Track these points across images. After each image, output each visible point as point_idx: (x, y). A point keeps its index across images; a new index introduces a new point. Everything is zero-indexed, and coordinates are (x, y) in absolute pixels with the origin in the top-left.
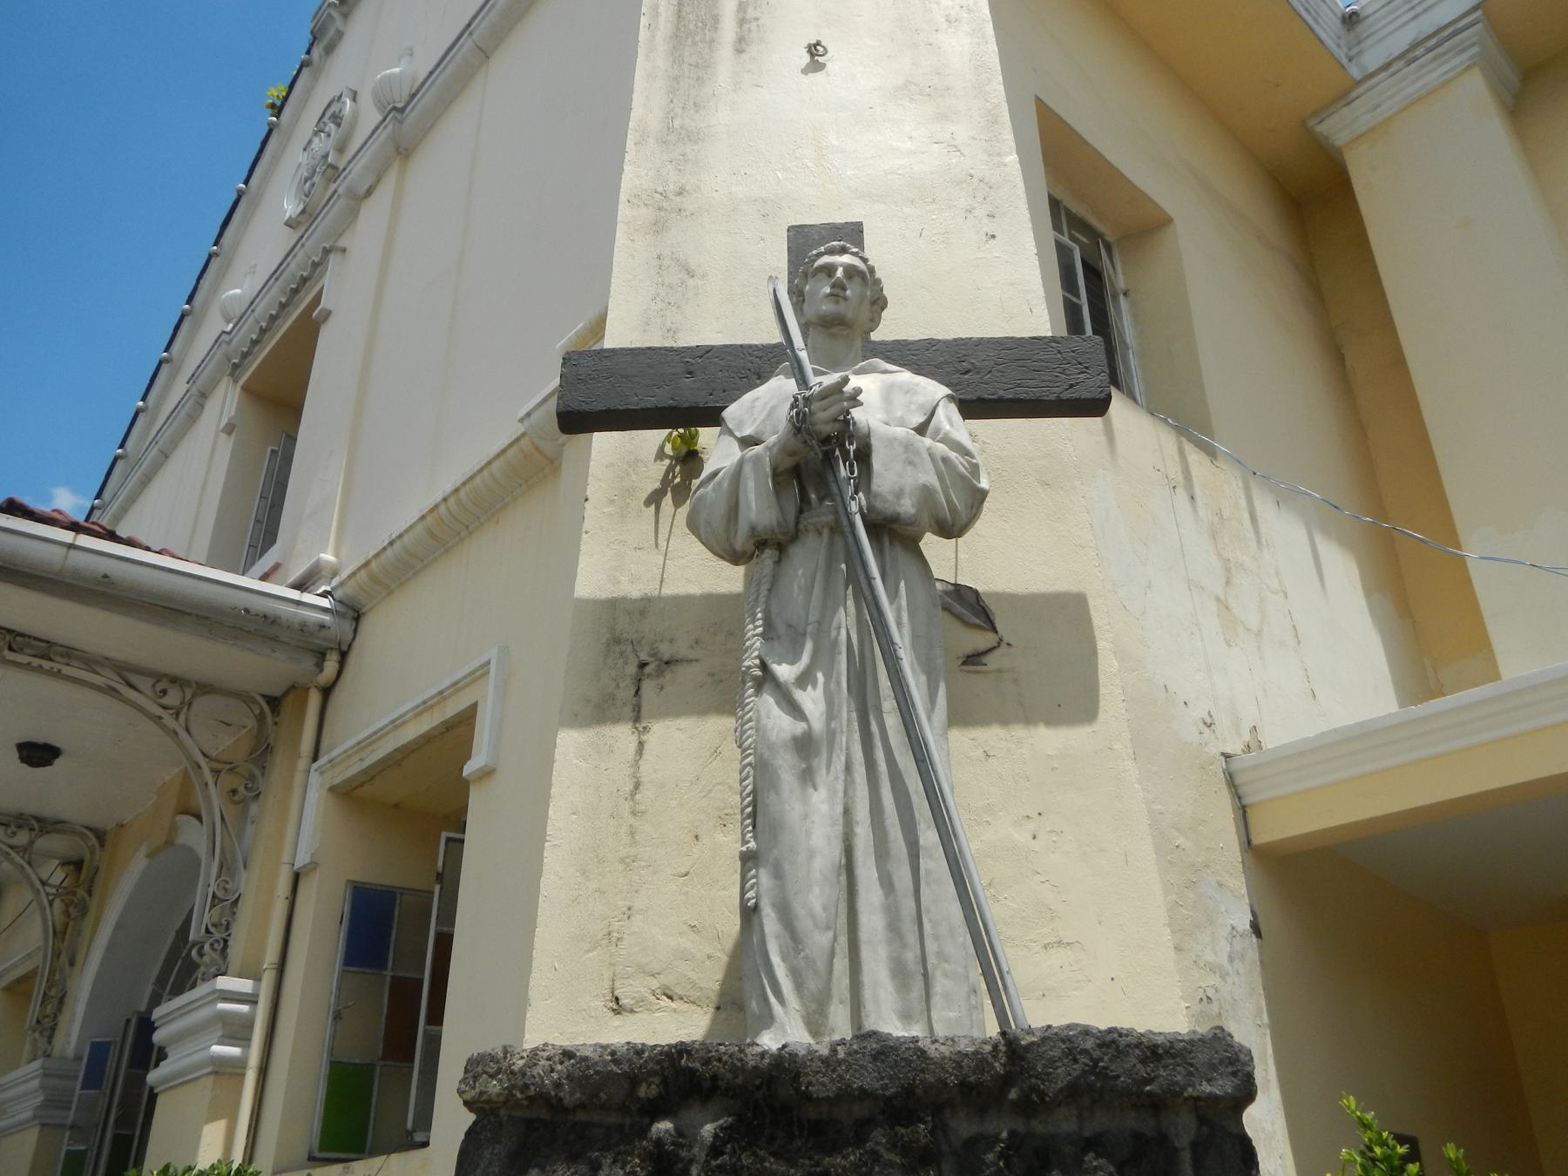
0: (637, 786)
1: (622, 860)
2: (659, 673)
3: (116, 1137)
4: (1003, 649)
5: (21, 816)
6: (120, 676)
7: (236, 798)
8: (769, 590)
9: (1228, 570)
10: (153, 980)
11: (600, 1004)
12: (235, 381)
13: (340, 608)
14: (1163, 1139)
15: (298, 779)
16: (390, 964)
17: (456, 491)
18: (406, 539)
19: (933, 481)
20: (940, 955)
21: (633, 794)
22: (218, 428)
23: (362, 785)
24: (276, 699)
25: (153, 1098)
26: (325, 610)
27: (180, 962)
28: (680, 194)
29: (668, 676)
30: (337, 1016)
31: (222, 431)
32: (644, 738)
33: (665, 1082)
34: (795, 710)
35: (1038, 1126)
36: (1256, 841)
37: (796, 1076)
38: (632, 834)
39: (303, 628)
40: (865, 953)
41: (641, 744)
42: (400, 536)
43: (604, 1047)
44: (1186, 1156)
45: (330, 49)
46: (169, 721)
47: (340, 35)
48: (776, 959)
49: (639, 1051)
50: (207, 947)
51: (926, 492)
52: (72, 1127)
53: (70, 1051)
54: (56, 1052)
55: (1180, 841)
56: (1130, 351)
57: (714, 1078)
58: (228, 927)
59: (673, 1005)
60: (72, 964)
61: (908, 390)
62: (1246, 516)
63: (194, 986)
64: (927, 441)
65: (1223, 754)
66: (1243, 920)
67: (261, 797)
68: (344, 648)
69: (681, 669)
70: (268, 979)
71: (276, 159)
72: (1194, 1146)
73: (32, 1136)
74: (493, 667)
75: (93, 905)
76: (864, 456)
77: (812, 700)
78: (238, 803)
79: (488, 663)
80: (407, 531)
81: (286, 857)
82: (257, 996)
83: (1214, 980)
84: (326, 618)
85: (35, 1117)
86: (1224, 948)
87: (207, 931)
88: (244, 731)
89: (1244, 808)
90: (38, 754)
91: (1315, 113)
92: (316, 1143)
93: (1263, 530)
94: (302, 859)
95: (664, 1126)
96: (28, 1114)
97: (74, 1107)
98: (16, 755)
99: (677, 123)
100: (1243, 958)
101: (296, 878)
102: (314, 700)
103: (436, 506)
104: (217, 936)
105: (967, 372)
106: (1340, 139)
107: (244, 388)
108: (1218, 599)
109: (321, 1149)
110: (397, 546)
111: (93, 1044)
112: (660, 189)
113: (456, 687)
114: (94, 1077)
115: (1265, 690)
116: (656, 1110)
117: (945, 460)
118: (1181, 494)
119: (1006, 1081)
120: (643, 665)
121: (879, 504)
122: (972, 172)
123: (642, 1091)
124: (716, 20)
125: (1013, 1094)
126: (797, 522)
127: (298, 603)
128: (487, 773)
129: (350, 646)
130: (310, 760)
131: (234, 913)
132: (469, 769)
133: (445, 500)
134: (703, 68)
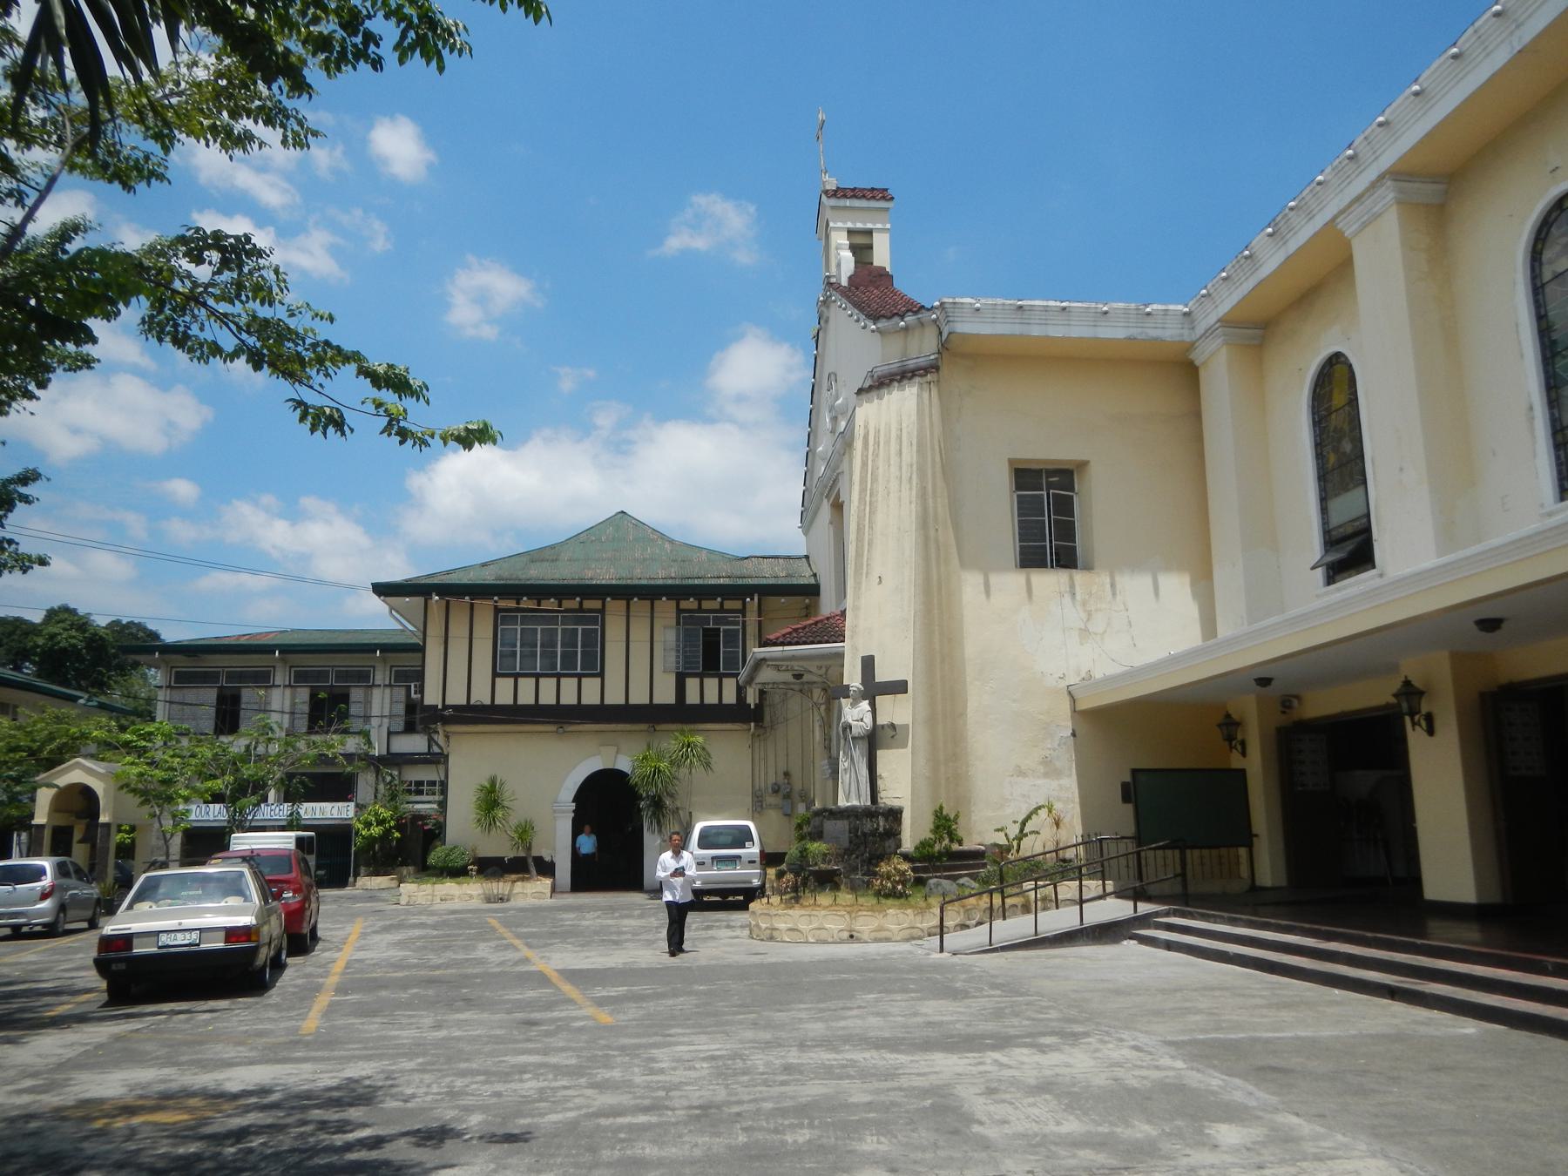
36: (1077, 709)
45: (827, 321)
47: (828, 318)
55: (1041, 717)
62: (1108, 586)
71: (822, 366)
89: (1074, 701)
91: (1187, 350)
93: (1118, 587)
100: (1065, 744)
106: (1197, 363)
118: (1067, 598)
124: (862, 564)
134: (860, 583)
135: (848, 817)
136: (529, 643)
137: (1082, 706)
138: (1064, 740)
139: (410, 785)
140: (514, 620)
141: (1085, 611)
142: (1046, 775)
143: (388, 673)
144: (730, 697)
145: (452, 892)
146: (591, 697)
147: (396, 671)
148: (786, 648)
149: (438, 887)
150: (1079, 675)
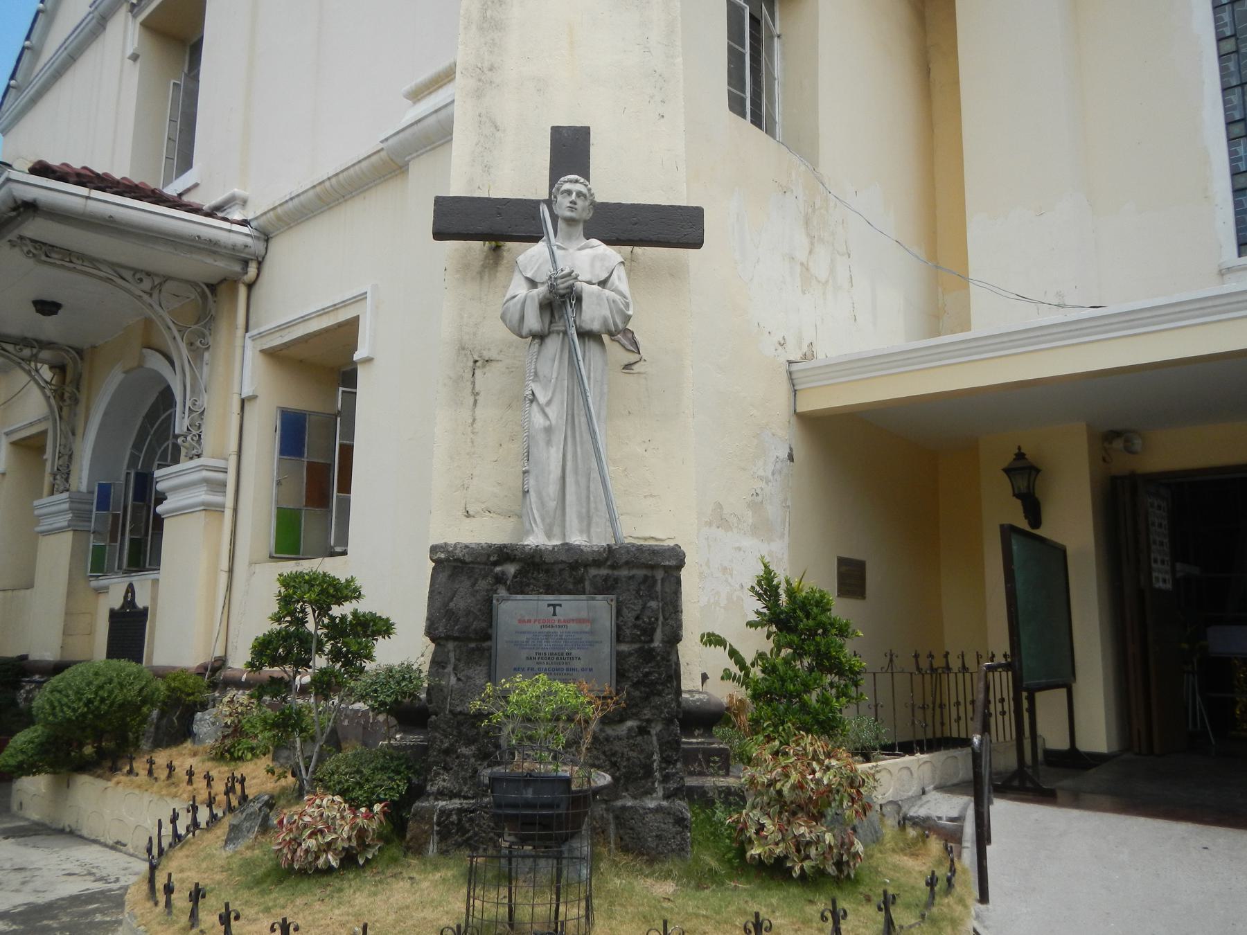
0: (474, 420)
1: (468, 454)
2: (484, 366)
3: (131, 540)
4: (641, 363)
5: (25, 339)
6: (116, 272)
7: (192, 347)
8: (537, 359)
9: (812, 244)
10: (130, 446)
11: (461, 513)
12: (135, 17)
13: (256, 233)
14: (653, 577)
15: (239, 342)
16: (306, 455)
17: (337, 174)
18: (302, 197)
19: (608, 314)
20: (596, 509)
21: (472, 424)
22: (123, 51)
23: (281, 350)
24: (212, 285)
25: (159, 522)
26: (247, 235)
27: (150, 437)
28: (490, 70)
29: (488, 368)
30: (279, 483)
31: (130, 58)
32: (477, 398)
33: (499, 556)
34: (546, 415)
35: (616, 573)
36: (798, 411)
37: (541, 557)
38: (472, 442)
39: (234, 247)
40: (568, 510)
41: (476, 401)
42: (298, 195)
43: (479, 544)
44: (659, 582)
46: (146, 297)
48: (535, 511)
49: (490, 546)
50: (189, 438)
51: (605, 321)
52: (94, 532)
53: (84, 488)
54: (73, 488)
56: (776, 82)
57: (515, 555)
58: (199, 427)
59: (491, 515)
60: (74, 434)
61: (603, 258)
63: (176, 460)
64: (606, 292)
65: (788, 361)
66: (784, 454)
67: (211, 349)
68: (260, 259)
69: (493, 364)
70: (233, 459)
72: (662, 579)
73: (68, 537)
74: (369, 295)
75: (83, 397)
76: (579, 299)
77: (552, 412)
78: (194, 351)
79: (366, 293)
80: (303, 193)
81: (236, 389)
82: (227, 469)
83: (763, 484)
84: (249, 241)
85: (69, 526)
86: (770, 468)
87: (188, 429)
88: (188, 300)
90: (47, 307)
92: (273, 550)
94: (247, 392)
95: (498, 569)
96: (66, 524)
97: (93, 520)
98: (33, 309)
99: (489, 13)
101: (243, 402)
102: (242, 291)
103: (323, 182)
104: (194, 432)
105: (636, 224)
107: (143, 24)
108: (802, 264)
109: (276, 552)
110: (296, 201)
111: (100, 485)
112: (479, 65)
113: (345, 304)
114: (103, 503)
115: (823, 319)
116: (496, 564)
117: (614, 301)
119: (607, 559)
120: (476, 362)
121: (584, 325)
122: (656, 69)
123: (492, 559)
125: (609, 563)
126: (549, 329)
127: (230, 231)
128: (368, 360)
129: (263, 258)
130: (244, 331)
131: (202, 419)
132: (357, 357)
133: (329, 179)
135: (606, 587)
137: (806, 406)
138: (778, 466)
141: (808, 235)
142: (755, 530)
148: (96, 194)
150: (800, 348)
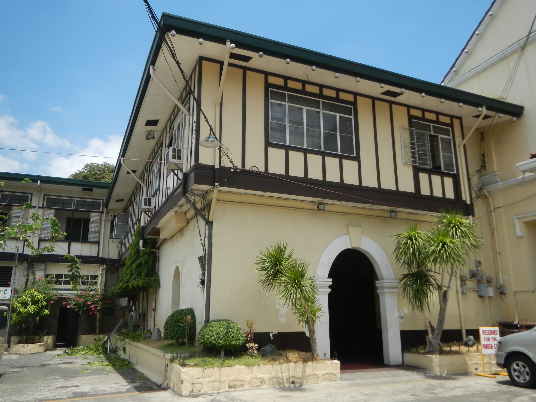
136: (296, 123)
139: (53, 278)
140: (282, 97)
143: (42, 199)
144: (450, 194)
145: (242, 377)
146: (351, 179)
147: (47, 198)
149: (226, 370)
